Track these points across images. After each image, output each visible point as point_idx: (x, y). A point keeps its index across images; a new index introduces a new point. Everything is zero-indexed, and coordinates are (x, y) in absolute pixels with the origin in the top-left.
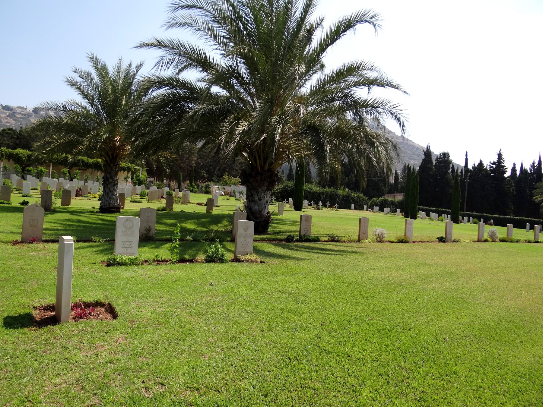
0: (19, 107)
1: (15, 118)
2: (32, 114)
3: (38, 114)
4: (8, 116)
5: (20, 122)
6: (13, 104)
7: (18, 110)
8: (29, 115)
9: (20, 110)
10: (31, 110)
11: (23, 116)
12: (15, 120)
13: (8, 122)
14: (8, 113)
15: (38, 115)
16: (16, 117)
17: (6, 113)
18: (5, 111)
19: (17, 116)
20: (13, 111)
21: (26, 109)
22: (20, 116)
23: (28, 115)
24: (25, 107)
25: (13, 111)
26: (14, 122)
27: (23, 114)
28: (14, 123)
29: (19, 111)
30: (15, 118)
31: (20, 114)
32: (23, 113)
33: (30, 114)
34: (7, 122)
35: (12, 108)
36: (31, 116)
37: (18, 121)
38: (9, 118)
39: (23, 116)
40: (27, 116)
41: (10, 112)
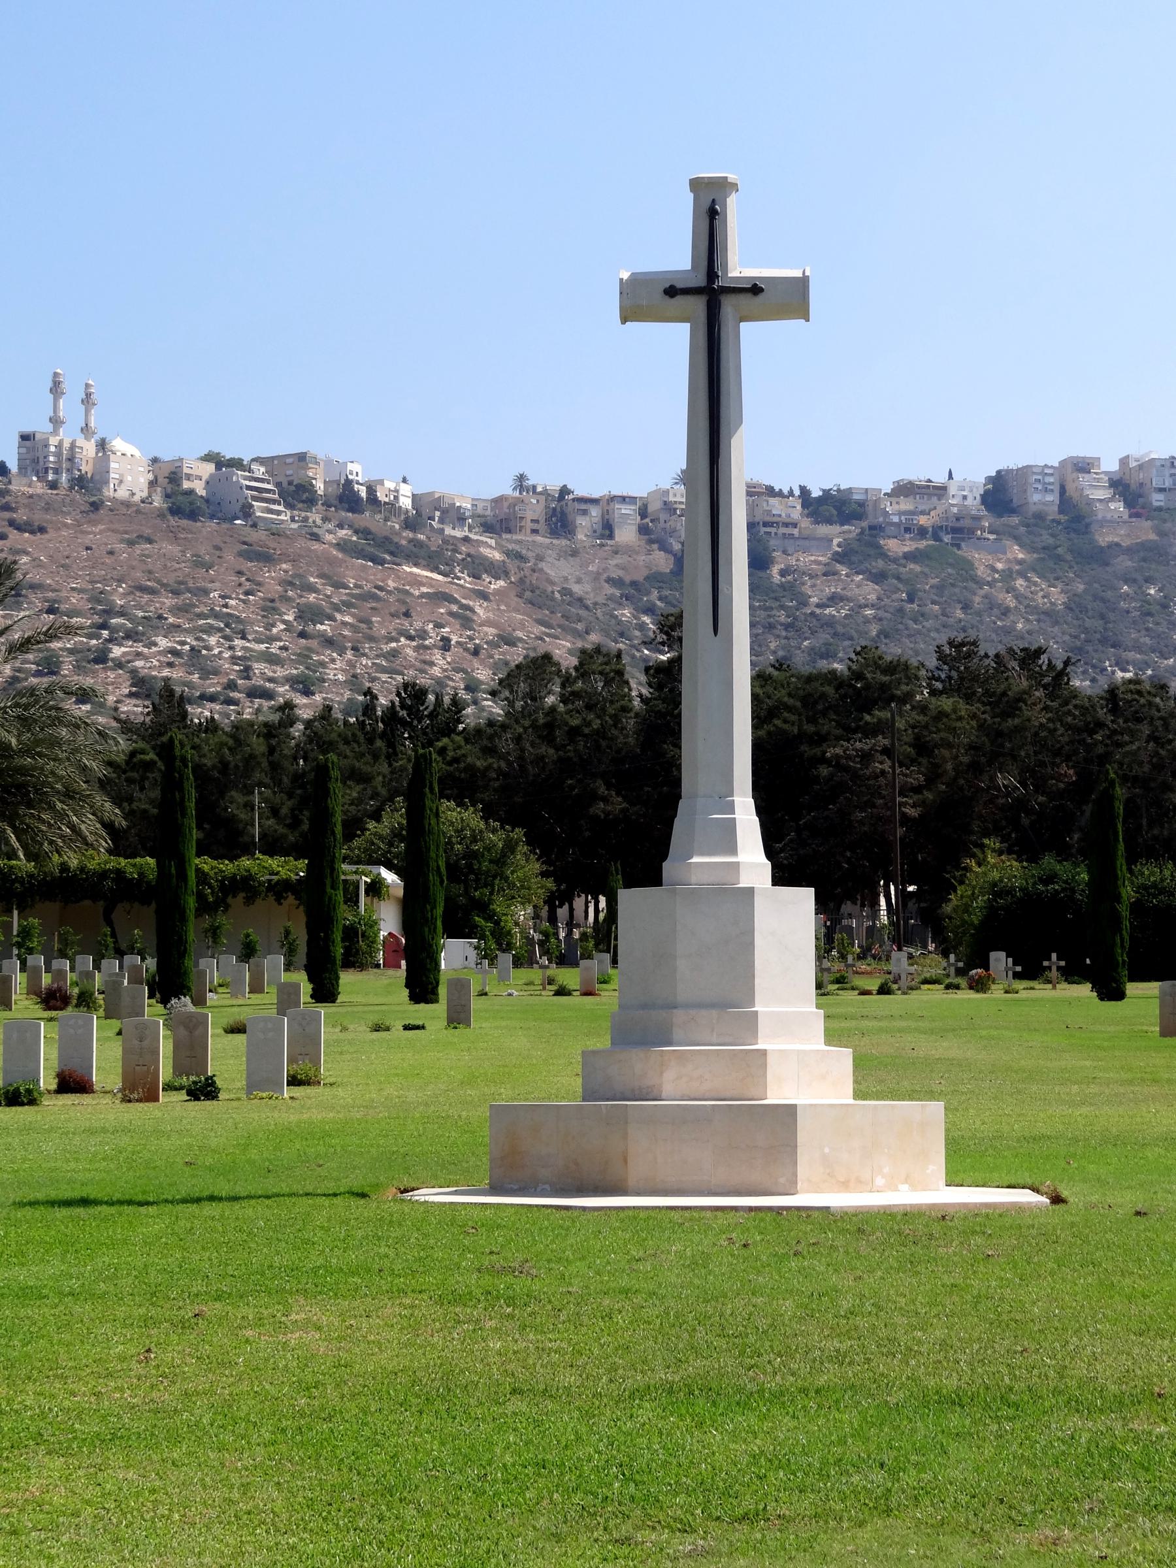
0: (904, 489)
2: (977, 519)
3: (1013, 511)
4: (839, 558)
5: (905, 582)
9: (906, 504)
10: (973, 502)
11: (922, 544)
12: (878, 578)
13: (842, 599)
14: (837, 535)
15: (1015, 520)
16: (883, 555)
18: (824, 530)
19: (895, 546)
20: (865, 524)
21: (941, 491)
22: (909, 546)
23: (955, 530)
24: (940, 478)
25: (865, 524)
26: (870, 591)
27: (922, 532)
28: (873, 597)
29: (900, 513)
30: (880, 563)
31: (907, 530)
32: (923, 520)
33: (966, 523)
34: (834, 599)
35: (861, 504)
36: (972, 531)
37: (898, 578)
38: (844, 571)
39: (922, 544)
40: (947, 539)
41: (852, 530)
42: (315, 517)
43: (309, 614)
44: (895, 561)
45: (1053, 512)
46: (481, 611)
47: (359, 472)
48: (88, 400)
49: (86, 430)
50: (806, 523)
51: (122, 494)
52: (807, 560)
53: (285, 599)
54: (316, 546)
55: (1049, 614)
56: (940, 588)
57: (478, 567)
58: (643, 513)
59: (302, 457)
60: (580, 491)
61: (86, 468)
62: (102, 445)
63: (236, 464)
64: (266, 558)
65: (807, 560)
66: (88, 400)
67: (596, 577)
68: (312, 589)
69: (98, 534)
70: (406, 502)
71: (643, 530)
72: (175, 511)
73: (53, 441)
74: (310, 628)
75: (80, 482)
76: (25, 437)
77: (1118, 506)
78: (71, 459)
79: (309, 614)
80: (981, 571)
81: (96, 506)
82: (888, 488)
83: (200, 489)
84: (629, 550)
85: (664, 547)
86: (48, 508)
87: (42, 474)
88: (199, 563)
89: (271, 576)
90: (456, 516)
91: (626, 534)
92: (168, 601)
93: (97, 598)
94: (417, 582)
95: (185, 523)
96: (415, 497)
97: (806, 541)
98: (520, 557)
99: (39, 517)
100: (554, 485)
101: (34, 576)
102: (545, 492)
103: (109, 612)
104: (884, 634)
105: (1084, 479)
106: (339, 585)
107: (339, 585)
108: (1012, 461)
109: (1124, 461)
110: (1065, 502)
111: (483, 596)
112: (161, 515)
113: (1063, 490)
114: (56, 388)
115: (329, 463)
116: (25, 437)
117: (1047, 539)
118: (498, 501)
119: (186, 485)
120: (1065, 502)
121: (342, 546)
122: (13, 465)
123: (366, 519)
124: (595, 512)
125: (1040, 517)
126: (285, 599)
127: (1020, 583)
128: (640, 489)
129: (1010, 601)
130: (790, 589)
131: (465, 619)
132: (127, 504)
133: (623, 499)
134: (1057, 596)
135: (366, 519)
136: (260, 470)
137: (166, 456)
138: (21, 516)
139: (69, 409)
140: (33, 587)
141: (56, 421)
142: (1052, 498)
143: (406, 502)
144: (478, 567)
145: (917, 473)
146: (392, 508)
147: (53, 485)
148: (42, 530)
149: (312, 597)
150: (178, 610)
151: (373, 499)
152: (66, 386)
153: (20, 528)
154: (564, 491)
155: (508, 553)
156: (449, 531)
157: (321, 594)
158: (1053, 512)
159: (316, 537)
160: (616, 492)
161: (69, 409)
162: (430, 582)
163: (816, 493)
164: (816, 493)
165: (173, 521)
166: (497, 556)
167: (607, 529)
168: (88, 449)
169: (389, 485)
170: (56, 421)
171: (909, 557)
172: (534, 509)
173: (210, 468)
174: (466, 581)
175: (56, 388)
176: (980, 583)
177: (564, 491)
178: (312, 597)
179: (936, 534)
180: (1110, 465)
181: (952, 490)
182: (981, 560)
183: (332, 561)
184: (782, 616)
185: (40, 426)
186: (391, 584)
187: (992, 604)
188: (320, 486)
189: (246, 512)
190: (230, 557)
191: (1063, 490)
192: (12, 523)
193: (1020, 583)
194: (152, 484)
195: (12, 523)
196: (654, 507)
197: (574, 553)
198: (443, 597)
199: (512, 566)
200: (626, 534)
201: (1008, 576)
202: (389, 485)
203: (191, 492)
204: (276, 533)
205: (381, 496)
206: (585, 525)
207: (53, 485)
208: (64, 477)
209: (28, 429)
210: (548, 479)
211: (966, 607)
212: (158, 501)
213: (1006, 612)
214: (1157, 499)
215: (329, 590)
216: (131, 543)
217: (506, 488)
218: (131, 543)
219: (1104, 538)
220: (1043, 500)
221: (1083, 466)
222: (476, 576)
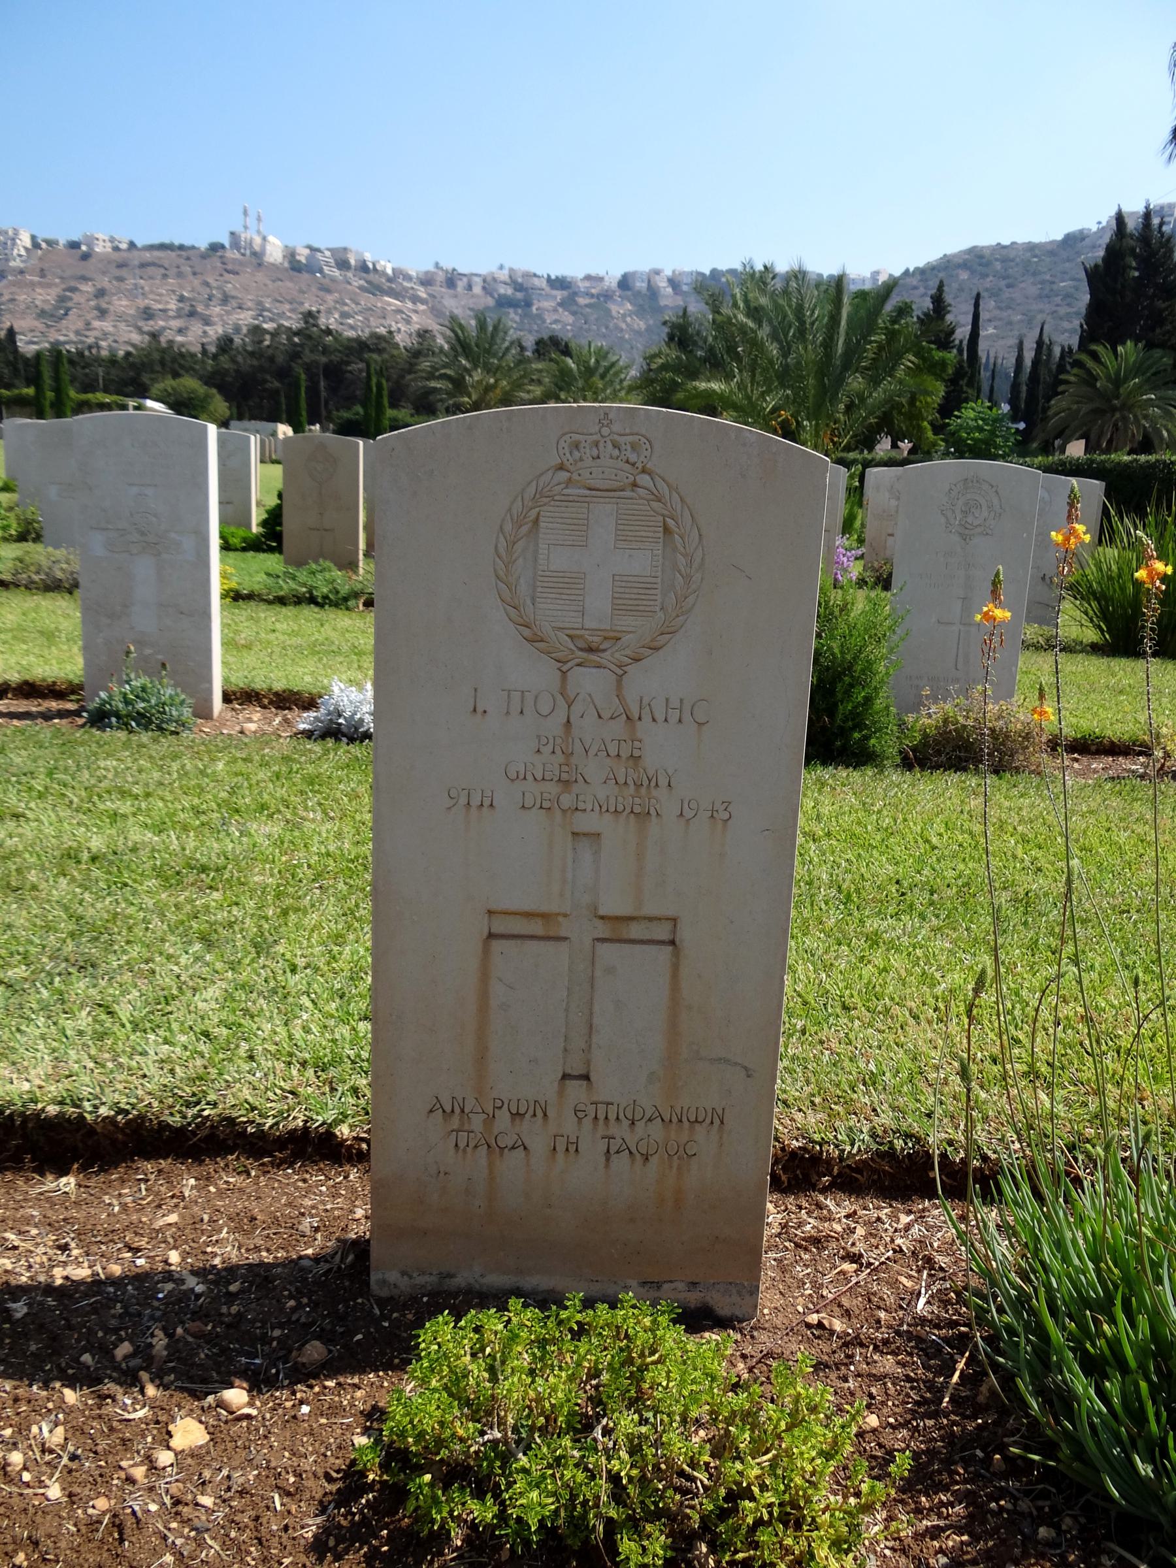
0: (588, 278)
1: (575, 308)
4: (560, 304)
6: (574, 269)
7: (582, 286)
8: (607, 296)
9: (587, 284)
10: (614, 285)
11: (592, 301)
12: (574, 313)
14: (559, 295)
15: (629, 293)
16: (576, 304)
17: (555, 297)
18: (555, 292)
19: (582, 301)
21: (601, 279)
22: (587, 301)
24: (602, 273)
26: (570, 319)
27: (592, 296)
30: (575, 308)
32: (593, 291)
33: (610, 293)
34: (556, 322)
38: (560, 310)
39: (592, 301)
41: (565, 293)
42: (350, 274)
43: (345, 315)
44: (581, 307)
45: (644, 291)
46: (415, 318)
47: (368, 257)
48: (259, 219)
49: (259, 232)
50: (548, 289)
51: (271, 260)
52: (547, 304)
53: (336, 308)
54: (349, 287)
55: (638, 333)
56: (597, 320)
57: (415, 299)
58: (484, 281)
59: (345, 249)
60: (461, 270)
61: (257, 248)
62: (264, 239)
63: (318, 250)
64: (328, 291)
65: (547, 304)
66: (259, 219)
67: (463, 307)
68: (346, 305)
69: (260, 276)
70: (389, 271)
71: (484, 288)
72: (293, 269)
73: (243, 236)
74: (344, 321)
75: (254, 254)
76: (232, 234)
77: (670, 290)
78: (251, 244)
79: (345, 315)
80: (614, 313)
81: (260, 265)
82: (581, 275)
83: (303, 260)
84: (477, 296)
85: (492, 296)
86: (241, 264)
87: (238, 249)
88: (302, 292)
89: (330, 298)
90: (408, 278)
91: (477, 290)
92: (288, 306)
93: (260, 303)
94: (389, 304)
95: (296, 274)
96: (393, 270)
97: (548, 297)
98: (434, 297)
99: (237, 268)
100: (450, 268)
101: (234, 293)
102: (447, 272)
103: (264, 309)
104: (574, 336)
105: (657, 277)
106: (358, 304)
107: (358, 304)
108: (630, 268)
109: (674, 272)
110: (650, 286)
111: (416, 312)
112: (286, 270)
113: (649, 281)
114: (245, 213)
115: (357, 252)
116: (232, 234)
117: (641, 302)
118: (427, 273)
119: (298, 258)
120: (650, 286)
121: (361, 288)
122: (227, 245)
123: (372, 277)
124: (465, 280)
125: (639, 292)
126: (336, 308)
127: (628, 319)
128: (483, 271)
129: (624, 326)
130: (540, 317)
131: (408, 321)
132: (273, 265)
133: (476, 275)
134: (642, 325)
135: (372, 277)
136: (328, 253)
137: (290, 245)
138: (229, 267)
139: (251, 221)
140: (233, 297)
141: (246, 227)
142: (645, 285)
143: (389, 271)
144: (415, 299)
145: (593, 272)
146: (384, 273)
147: (243, 255)
148: (237, 273)
149: (346, 308)
150: (292, 311)
151: (375, 269)
152: (249, 212)
153: (228, 272)
154: (454, 270)
155: (429, 295)
156: (406, 284)
157: (350, 307)
158: (644, 291)
159: (349, 283)
160: (474, 272)
161: (251, 221)
162: (395, 305)
163: (553, 277)
164: (553, 277)
165: (291, 272)
166: (424, 296)
167: (469, 287)
168: (258, 240)
169: (383, 263)
170: (246, 227)
171: (586, 306)
172: (441, 277)
173: (307, 251)
174: (410, 305)
175: (245, 213)
176: (613, 318)
177: (454, 270)
178: (346, 308)
179: (598, 296)
180: (668, 272)
181: (606, 279)
182: (614, 309)
183: (355, 293)
184: (535, 327)
185: (238, 229)
186: (379, 305)
187: (617, 328)
188: (353, 262)
189: (321, 271)
190: (314, 290)
191: (649, 281)
192: (226, 270)
193: (628, 319)
194: (284, 257)
195: (226, 270)
196: (489, 279)
197: (456, 296)
198: (400, 311)
199: (430, 300)
200: (477, 290)
201: (624, 316)
202: (383, 263)
203: (299, 262)
204: (333, 280)
205: (378, 267)
206: (461, 285)
207: (243, 255)
208: (248, 252)
209: (233, 229)
210: (447, 264)
211: (607, 328)
212: (286, 265)
213: (622, 330)
214: (685, 288)
215: (353, 306)
216: (274, 281)
217: (431, 268)
218: (274, 281)
219: (663, 302)
220: (641, 285)
221: (657, 272)
222: (414, 303)
